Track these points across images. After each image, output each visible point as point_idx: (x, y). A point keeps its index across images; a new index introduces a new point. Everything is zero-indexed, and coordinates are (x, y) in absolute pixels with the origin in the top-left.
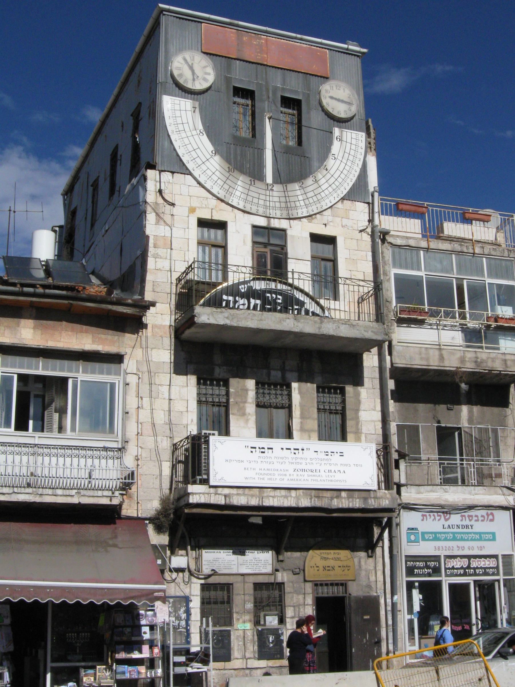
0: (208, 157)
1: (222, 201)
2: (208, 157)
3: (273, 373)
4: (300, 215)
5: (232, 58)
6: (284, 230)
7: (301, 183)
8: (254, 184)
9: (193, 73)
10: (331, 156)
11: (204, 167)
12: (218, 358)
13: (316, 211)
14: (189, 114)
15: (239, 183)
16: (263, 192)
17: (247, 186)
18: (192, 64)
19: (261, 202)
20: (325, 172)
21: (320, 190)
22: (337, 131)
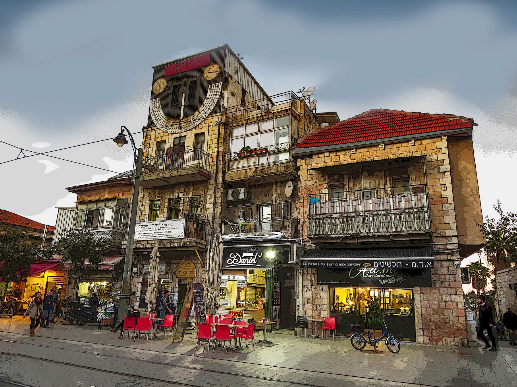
3: (175, 194)
6: (185, 136)
12: (157, 193)
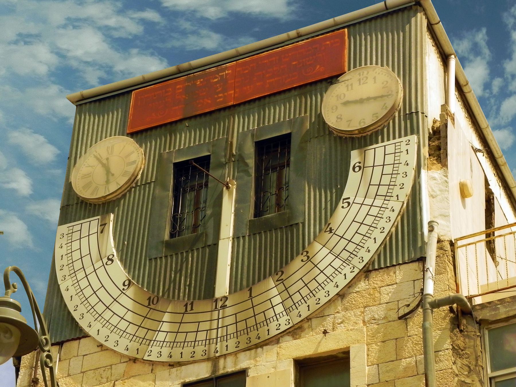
0: (115, 293)
1: (135, 360)
2: (115, 293)
4: (274, 332)
5: (176, 122)
6: (243, 373)
7: (280, 273)
8: (192, 309)
9: (108, 172)
10: (341, 204)
11: (108, 315)
13: (305, 314)
14: (93, 238)
15: (166, 317)
16: (207, 317)
17: (178, 318)
18: (107, 159)
19: (202, 336)
20: (328, 235)
21: (317, 271)
22: (355, 157)
